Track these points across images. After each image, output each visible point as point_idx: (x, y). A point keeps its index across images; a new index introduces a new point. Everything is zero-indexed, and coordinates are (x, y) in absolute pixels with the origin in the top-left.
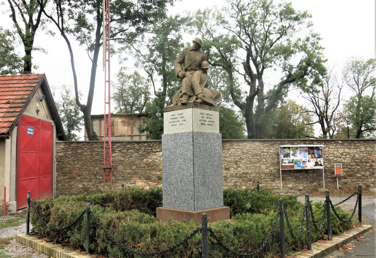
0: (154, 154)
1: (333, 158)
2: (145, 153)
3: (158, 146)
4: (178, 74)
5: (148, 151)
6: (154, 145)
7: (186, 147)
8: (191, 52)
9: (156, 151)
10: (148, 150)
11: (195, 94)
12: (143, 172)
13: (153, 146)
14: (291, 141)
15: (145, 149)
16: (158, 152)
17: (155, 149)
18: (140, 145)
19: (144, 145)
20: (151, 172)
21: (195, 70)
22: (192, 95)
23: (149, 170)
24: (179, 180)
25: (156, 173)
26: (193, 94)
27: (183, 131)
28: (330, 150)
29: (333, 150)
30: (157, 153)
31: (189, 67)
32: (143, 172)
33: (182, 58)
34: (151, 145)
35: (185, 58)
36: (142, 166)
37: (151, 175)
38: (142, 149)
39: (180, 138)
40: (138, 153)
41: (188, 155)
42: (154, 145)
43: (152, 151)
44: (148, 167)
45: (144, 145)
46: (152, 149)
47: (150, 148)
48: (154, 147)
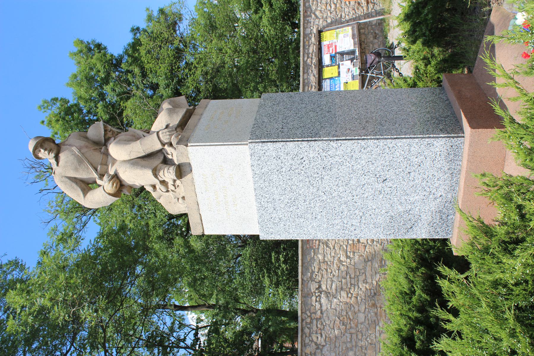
0: (325, 315)
1: (334, 4)
2: (323, 332)
3: (309, 306)
4: (109, 194)
5: (319, 326)
6: (309, 314)
7: (291, 162)
8: (60, 164)
9: (319, 311)
10: (317, 327)
11: (160, 151)
12: (360, 337)
13: (310, 316)
14: (303, 68)
15: (316, 333)
16: (321, 306)
17: (315, 313)
18: (307, 341)
19: (308, 335)
20: (360, 322)
21: (107, 154)
22: (162, 158)
23: (357, 326)
24: (379, 186)
25: (363, 311)
26: (159, 154)
27: (250, 174)
28: (319, 9)
29: (319, 4)
30: (324, 308)
31: (96, 170)
32: (360, 337)
33: (74, 185)
34: (308, 320)
35: (75, 178)
36: (349, 340)
37: (367, 322)
38: (315, 339)
39: (267, 184)
40: (323, 346)
41: (311, 156)
42: (309, 314)
43: (320, 318)
44: (351, 328)
45: (308, 335)
46: (317, 319)
47: (315, 322)
48: (313, 315)
